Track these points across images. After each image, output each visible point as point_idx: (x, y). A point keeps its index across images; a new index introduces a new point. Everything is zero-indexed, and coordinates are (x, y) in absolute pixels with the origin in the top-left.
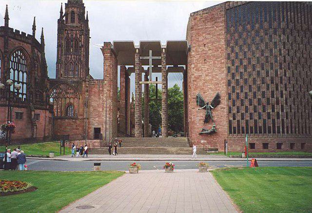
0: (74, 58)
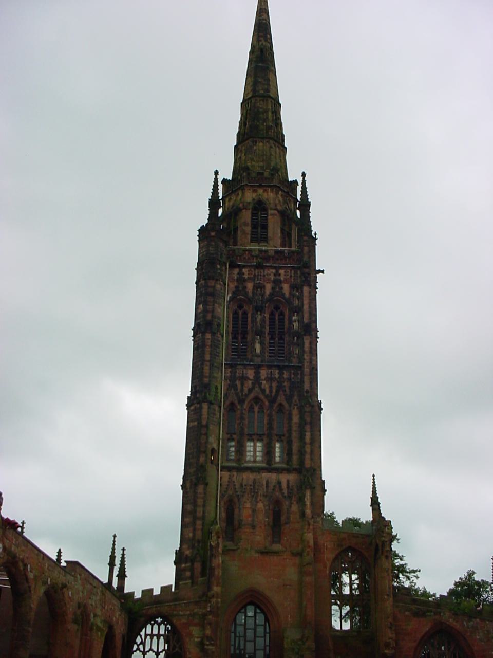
0: (270, 379)
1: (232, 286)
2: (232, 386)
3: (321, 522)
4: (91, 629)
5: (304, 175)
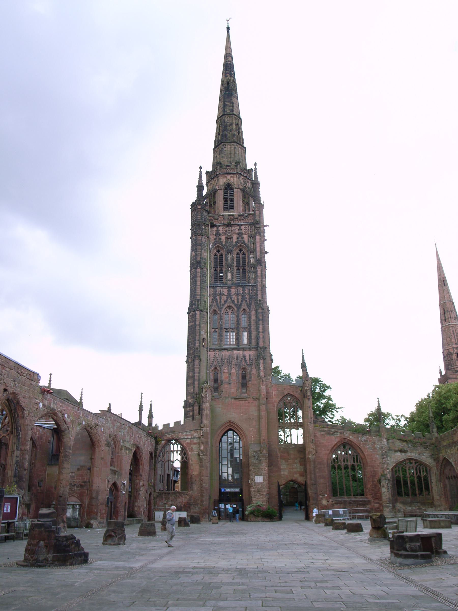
0: (237, 294)
1: (212, 238)
2: (215, 300)
3: (270, 379)
4: (121, 449)
5: (255, 164)
